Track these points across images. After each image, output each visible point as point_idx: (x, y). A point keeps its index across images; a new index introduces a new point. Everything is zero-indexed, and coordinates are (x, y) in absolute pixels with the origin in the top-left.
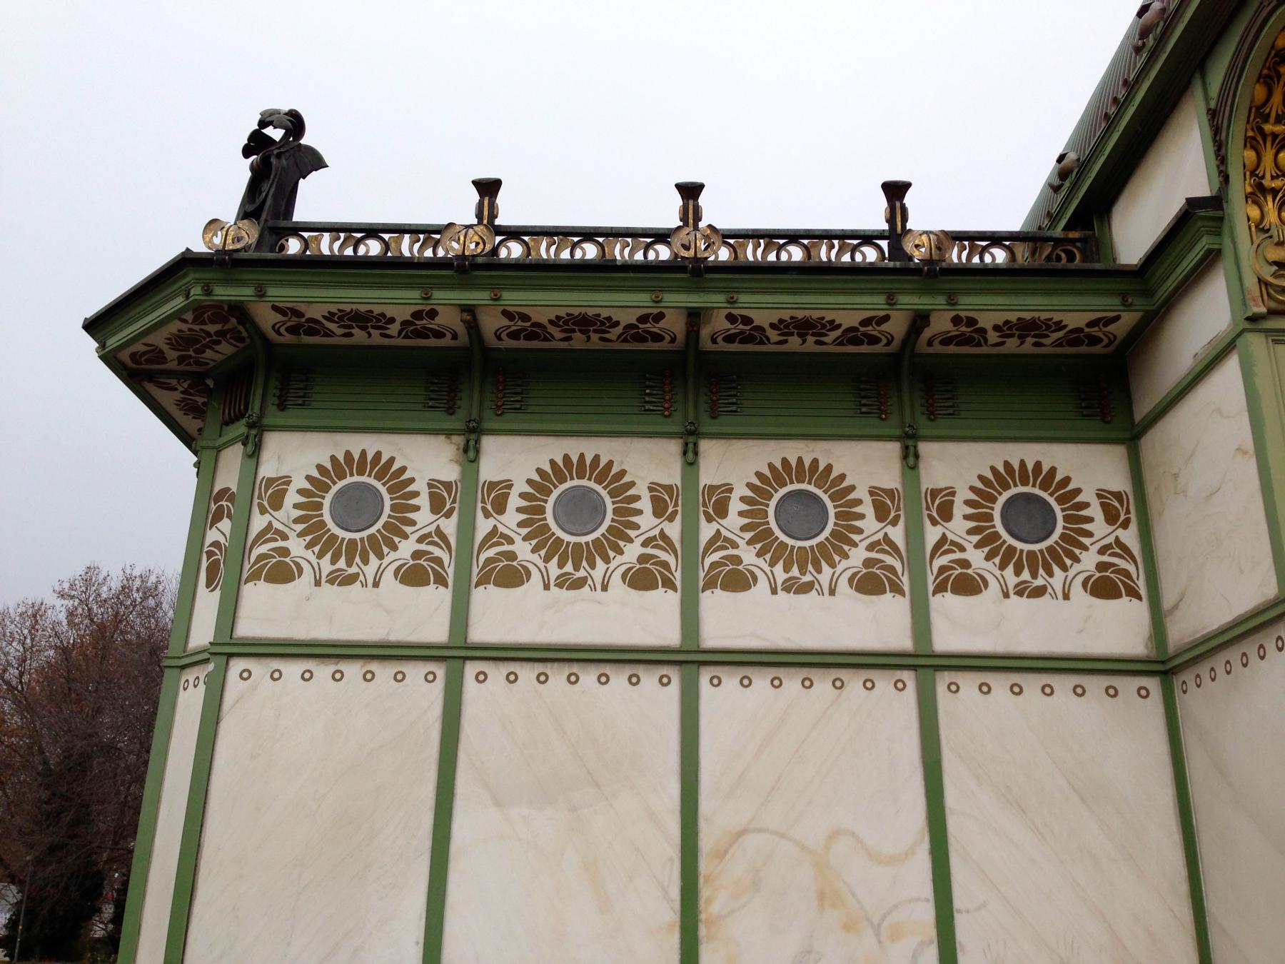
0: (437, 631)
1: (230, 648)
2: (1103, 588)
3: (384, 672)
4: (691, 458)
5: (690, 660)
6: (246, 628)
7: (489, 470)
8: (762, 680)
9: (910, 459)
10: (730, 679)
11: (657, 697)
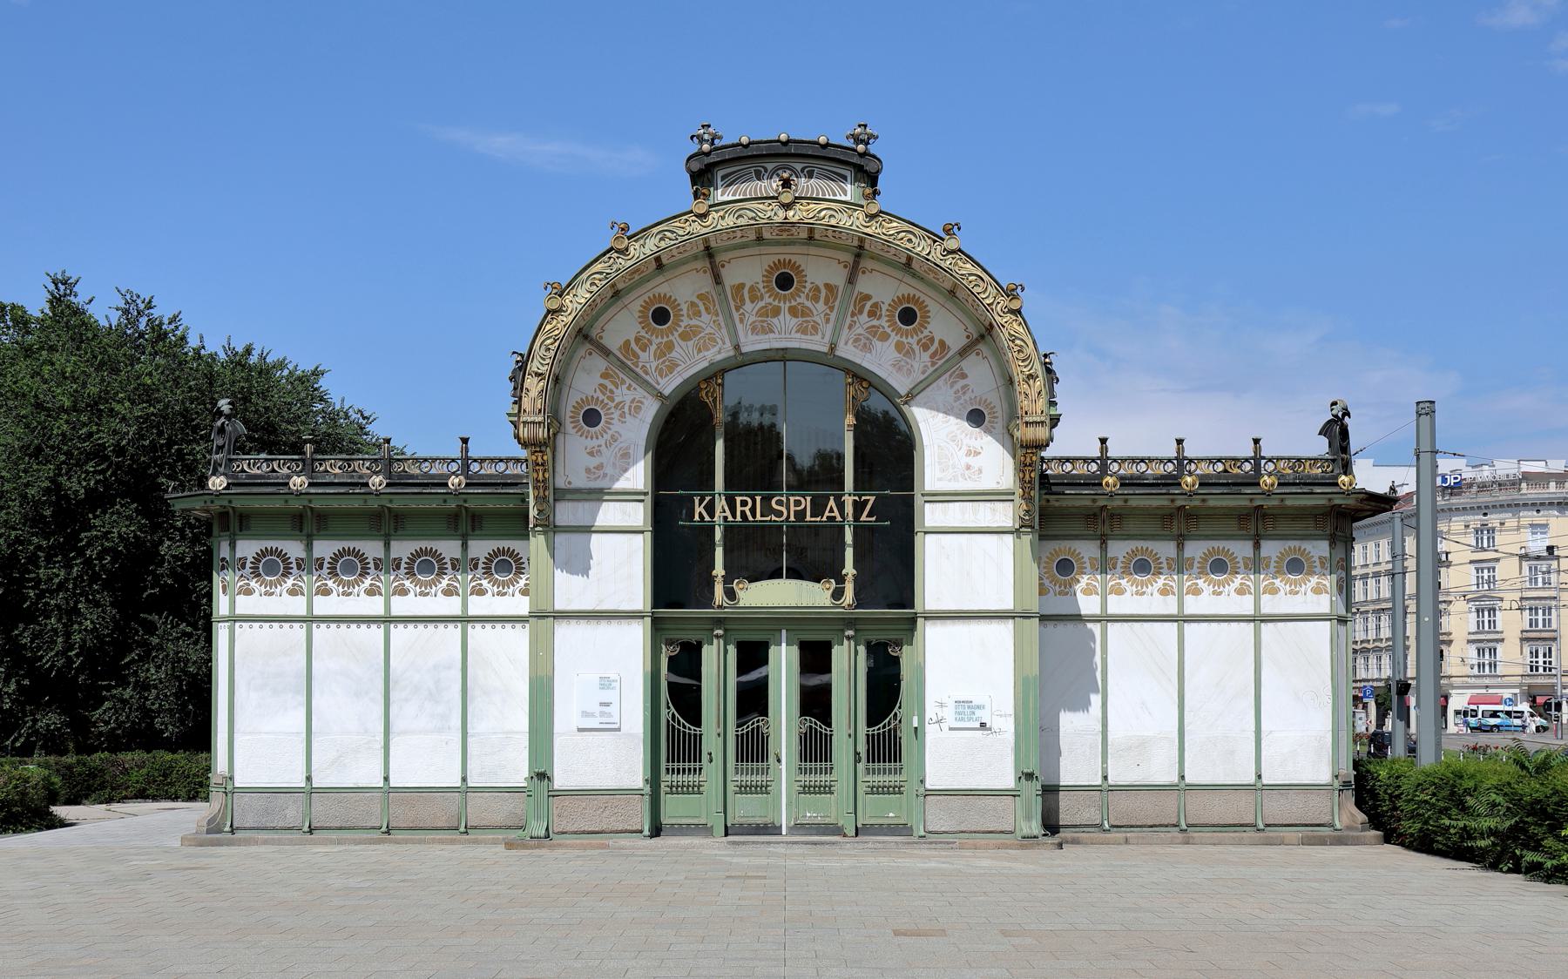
0: (303, 612)
1: (234, 619)
2: (525, 592)
3: (286, 625)
4: (387, 547)
5: (387, 620)
6: (238, 612)
7: (316, 555)
8: (411, 626)
9: (465, 547)
10: (401, 626)
11: (377, 632)
